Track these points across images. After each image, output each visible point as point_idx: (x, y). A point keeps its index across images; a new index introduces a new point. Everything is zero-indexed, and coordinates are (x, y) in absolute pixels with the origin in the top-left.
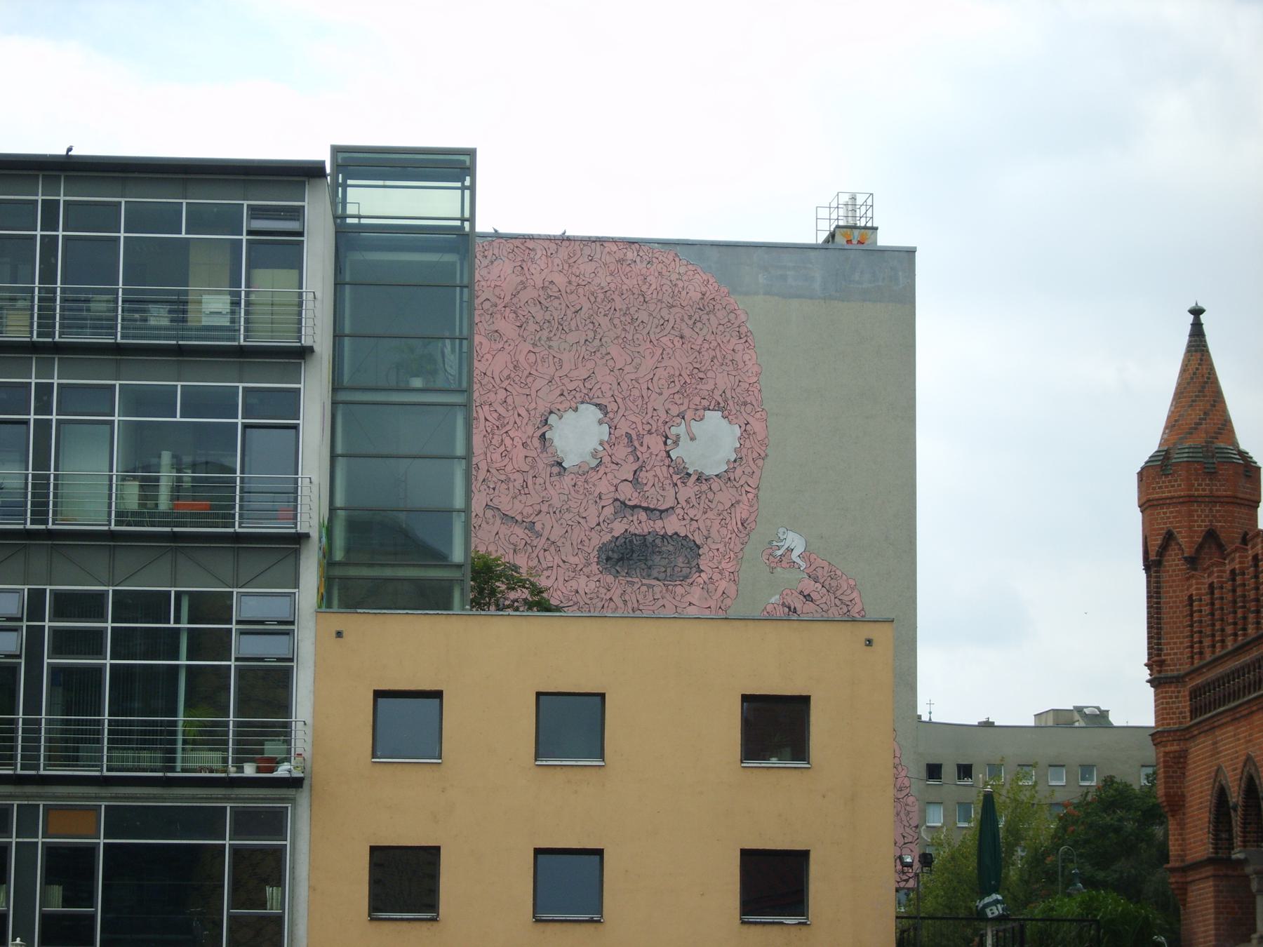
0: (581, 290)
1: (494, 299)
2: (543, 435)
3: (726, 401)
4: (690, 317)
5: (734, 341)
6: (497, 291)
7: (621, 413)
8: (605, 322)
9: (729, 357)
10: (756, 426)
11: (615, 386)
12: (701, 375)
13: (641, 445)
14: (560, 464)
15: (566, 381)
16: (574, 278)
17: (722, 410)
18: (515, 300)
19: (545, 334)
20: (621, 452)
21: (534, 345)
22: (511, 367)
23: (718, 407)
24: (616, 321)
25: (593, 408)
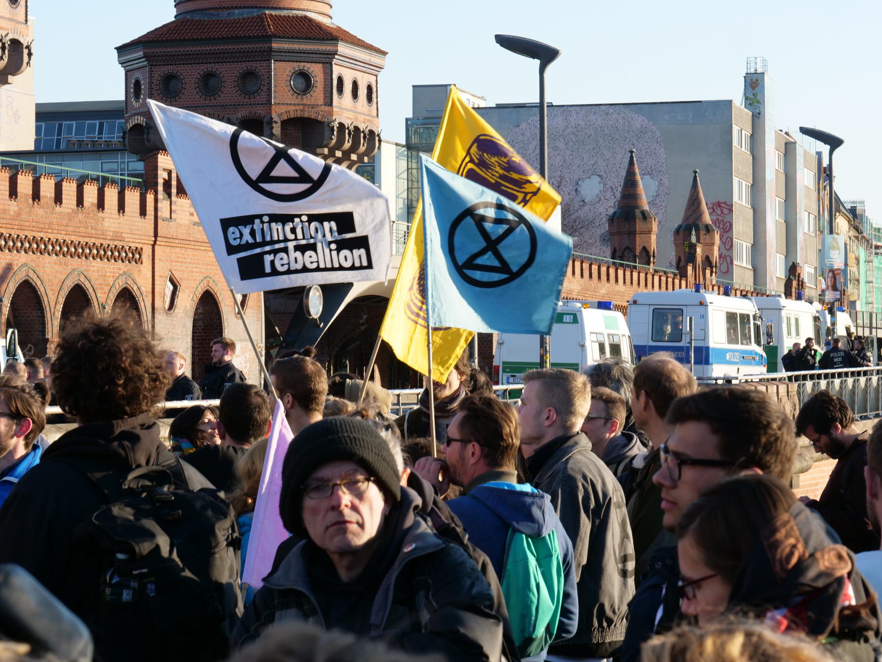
0: (591, 127)
1: (555, 133)
2: (576, 189)
3: (652, 171)
4: (637, 136)
5: (655, 145)
6: (557, 130)
7: (608, 178)
8: (601, 140)
9: (653, 152)
10: (665, 181)
11: (605, 166)
12: (642, 160)
13: (617, 191)
14: (583, 201)
15: (585, 166)
16: (588, 123)
17: (651, 174)
18: (564, 133)
19: (576, 147)
21: (572, 151)
22: (563, 161)
23: (649, 174)
24: (606, 139)
25: (597, 177)
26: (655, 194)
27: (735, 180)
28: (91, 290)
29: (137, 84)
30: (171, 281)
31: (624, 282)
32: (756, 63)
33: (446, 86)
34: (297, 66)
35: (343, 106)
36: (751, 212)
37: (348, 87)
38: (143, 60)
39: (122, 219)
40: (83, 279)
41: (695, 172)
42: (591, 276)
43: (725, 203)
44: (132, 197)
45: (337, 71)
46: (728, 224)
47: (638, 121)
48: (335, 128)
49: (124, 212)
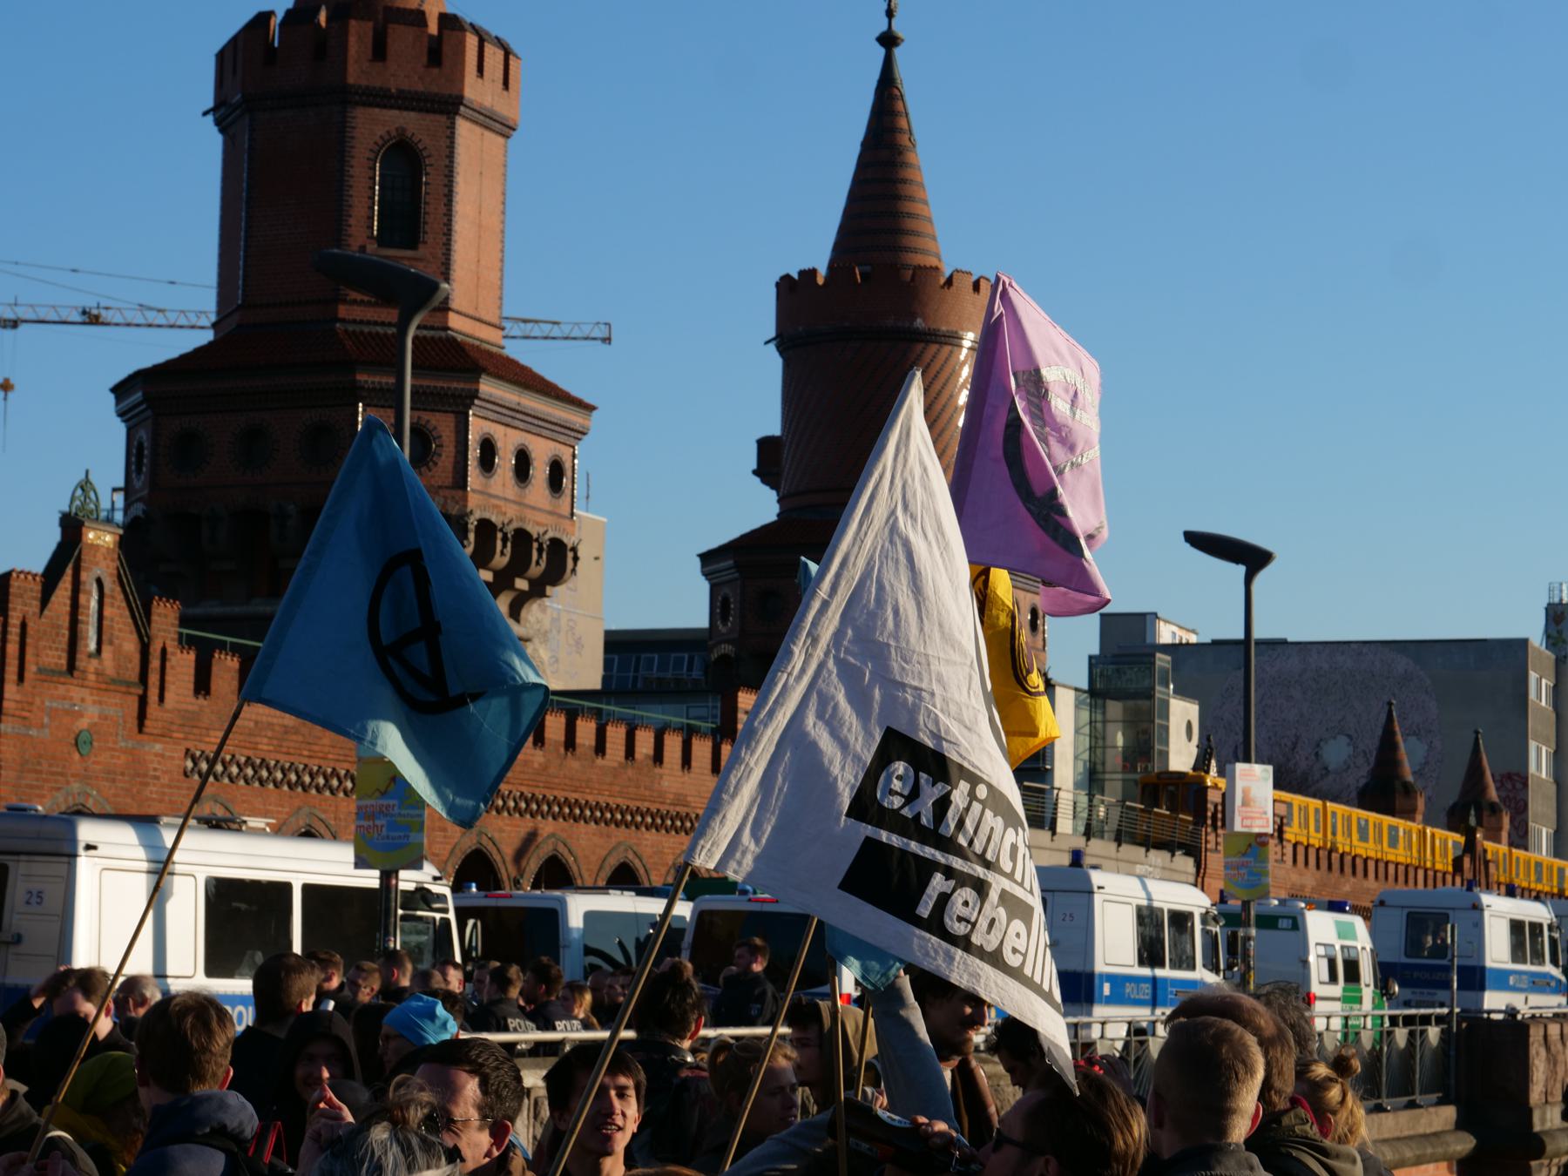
2: (1317, 754)
14: (1326, 768)
17: (1417, 735)
23: (1415, 734)
26: (1423, 761)
27: (1533, 745)
28: (642, 871)
29: (726, 602)
32: (1561, 591)
33: (1143, 616)
35: (526, 501)
36: (1554, 788)
38: (144, 406)
39: (687, 778)
40: (631, 856)
41: (1477, 733)
42: (1330, 867)
43: (1518, 775)
44: (702, 750)
46: (1522, 803)
47: (1402, 664)
48: (471, 527)
49: (689, 768)
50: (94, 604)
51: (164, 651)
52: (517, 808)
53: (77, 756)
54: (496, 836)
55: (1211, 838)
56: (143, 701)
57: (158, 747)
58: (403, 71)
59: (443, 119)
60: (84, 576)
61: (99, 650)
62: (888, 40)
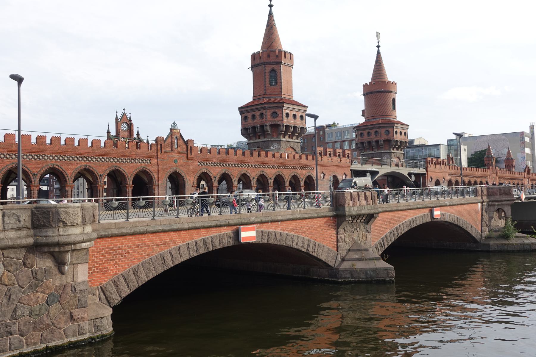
20: (497, 153)
30: (323, 173)
31: (469, 170)
34: (386, 129)
37: (399, 133)
40: (296, 174)
44: (310, 157)
45: (395, 130)
47: (503, 137)
50: (176, 141)
51: (191, 147)
52: (270, 167)
53: (174, 163)
54: (266, 172)
55: (429, 166)
56: (187, 154)
57: (192, 161)
58: (272, 59)
59: (279, 65)
60: (173, 137)
61: (177, 148)
62: (378, 47)
